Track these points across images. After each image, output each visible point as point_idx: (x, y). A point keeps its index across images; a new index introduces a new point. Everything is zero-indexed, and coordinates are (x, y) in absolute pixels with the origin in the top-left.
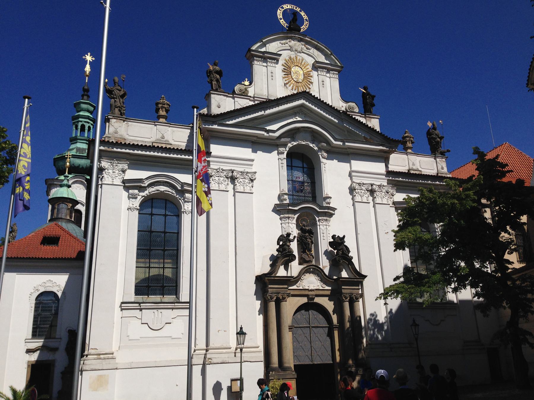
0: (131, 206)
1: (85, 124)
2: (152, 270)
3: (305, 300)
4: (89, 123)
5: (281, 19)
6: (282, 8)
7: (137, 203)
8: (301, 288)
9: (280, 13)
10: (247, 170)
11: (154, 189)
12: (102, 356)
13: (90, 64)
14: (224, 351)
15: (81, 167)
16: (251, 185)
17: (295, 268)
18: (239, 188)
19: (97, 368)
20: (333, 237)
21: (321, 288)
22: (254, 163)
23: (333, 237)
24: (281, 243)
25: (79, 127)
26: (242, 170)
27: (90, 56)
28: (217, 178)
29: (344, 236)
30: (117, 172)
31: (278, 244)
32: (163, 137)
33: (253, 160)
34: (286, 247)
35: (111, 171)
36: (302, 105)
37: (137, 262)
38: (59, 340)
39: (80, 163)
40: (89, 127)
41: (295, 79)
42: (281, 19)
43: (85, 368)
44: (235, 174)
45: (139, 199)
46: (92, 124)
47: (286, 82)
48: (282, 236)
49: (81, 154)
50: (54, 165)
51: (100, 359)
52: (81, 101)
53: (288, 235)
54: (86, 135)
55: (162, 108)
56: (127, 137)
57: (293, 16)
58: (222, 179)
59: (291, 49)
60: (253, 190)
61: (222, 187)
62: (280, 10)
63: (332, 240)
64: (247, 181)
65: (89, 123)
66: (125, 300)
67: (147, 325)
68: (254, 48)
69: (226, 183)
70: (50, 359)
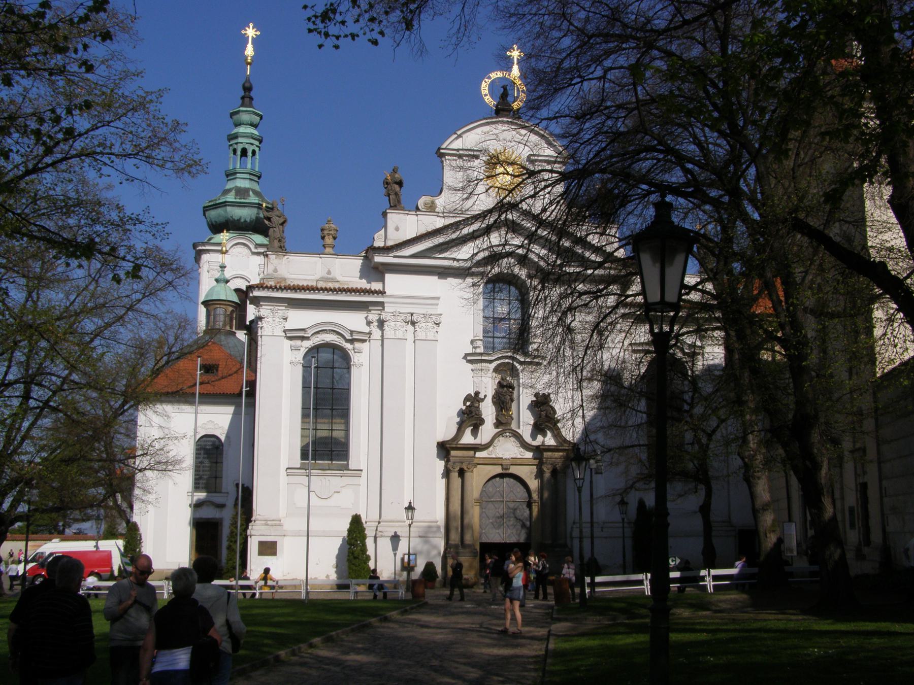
0: (294, 359)
1: (247, 146)
2: (318, 432)
3: (498, 470)
4: (252, 144)
5: (486, 95)
6: (490, 78)
7: (299, 356)
9: (485, 87)
10: (430, 312)
11: (318, 339)
12: (269, 522)
13: (253, 43)
14: (397, 524)
15: (242, 220)
16: (435, 330)
17: (488, 430)
18: (421, 334)
19: (265, 534)
20: (536, 395)
21: (519, 456)
22: (440, 302)
24: (468, 404)
25: (239, 153)
26: (424, 312)
27: (253, 28)
28: (392, 324)
30: (278, 320)
31: (465, 404)
32: (329, 273)
33: (438, 299)
34: (473, 409)
35: (270, 320)
37: (303, 422)
38: (225, 495)
39: (241, 215)
40: (254, 153)
42: (486, 95)
43: (253, 532)
44: (415, 318)
45: (303, 351)
46: (257, 146)
48: (469, 395)
49: (242, 201)
50: (204, 215)
51: (267, 525)
52: (241, 109)
53: (477, 394)
54: (249, 166)
55: (329, 235)
56: (286, 275)
57: (502, 90)
58: (399, 324)
60: (438, 337)
61: (400, 334)
62: (485, 82)
64: (430, 325)
65: (252, 144)
66: (290, 466)
68: (444, 146)
69: (405, 329)
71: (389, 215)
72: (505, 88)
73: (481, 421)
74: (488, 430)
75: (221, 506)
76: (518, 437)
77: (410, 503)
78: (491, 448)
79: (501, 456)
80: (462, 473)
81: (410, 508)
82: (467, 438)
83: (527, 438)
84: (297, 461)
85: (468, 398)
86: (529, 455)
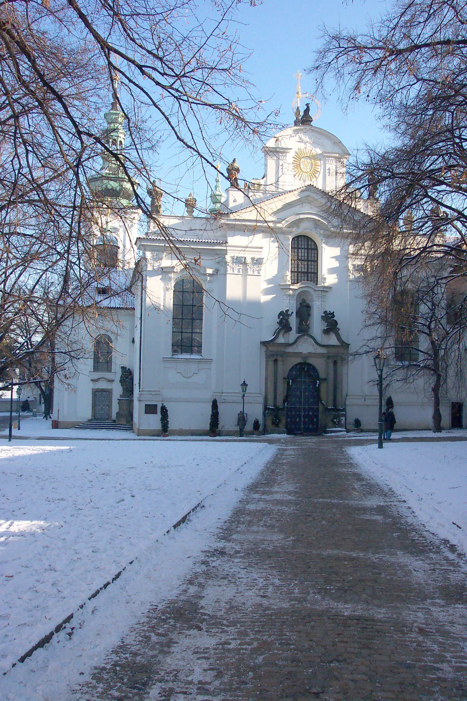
3: (300, 360)
8: (296, 351)
17: (293, 335)
20: (325, 312)
23: (325, 312)
24: (281, 317)
29: (333, 312)
31: (279, 317)
33: (262, 248)
36: (308, 196)
41: (304, 170)
47: (295, 173)
57: (306, 107)
59: (301, 141)
63: (324, 315)
67: (180, 374)
70: (109, 387)
71: (230, 192)
72: (307, 105)
73: (290, 329)
74: (293, 335)
75: (113, 381)
76: (314, 339)
77: (244, 381)
78: (295, 346)
79: (301, 351)
80: (276, 361)
81: (244, 384)
82: (281, 340)
83: (319, 340)
84: (169, 354)
85: (281, 313)
86: (320, 350)
